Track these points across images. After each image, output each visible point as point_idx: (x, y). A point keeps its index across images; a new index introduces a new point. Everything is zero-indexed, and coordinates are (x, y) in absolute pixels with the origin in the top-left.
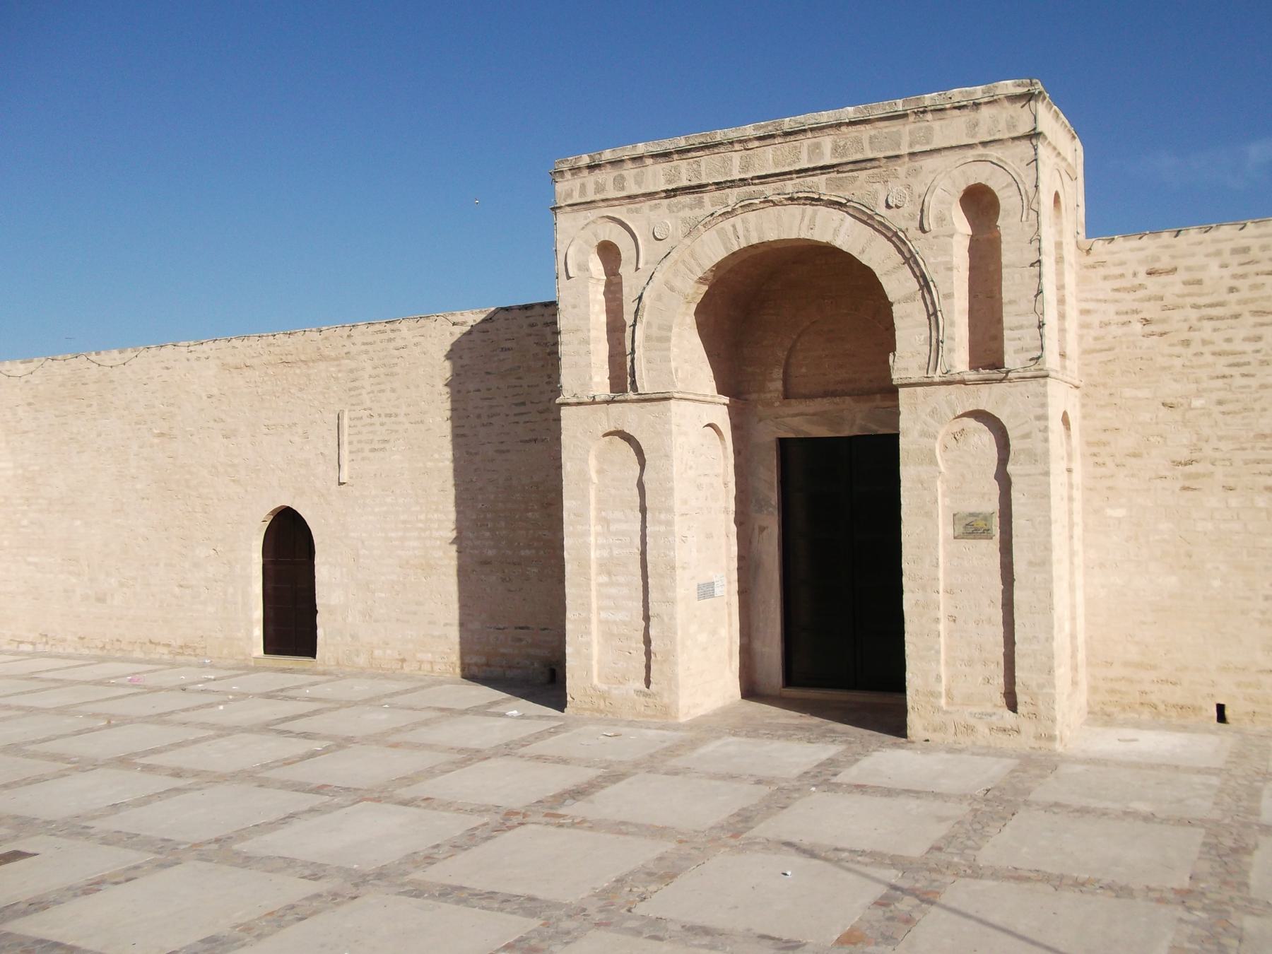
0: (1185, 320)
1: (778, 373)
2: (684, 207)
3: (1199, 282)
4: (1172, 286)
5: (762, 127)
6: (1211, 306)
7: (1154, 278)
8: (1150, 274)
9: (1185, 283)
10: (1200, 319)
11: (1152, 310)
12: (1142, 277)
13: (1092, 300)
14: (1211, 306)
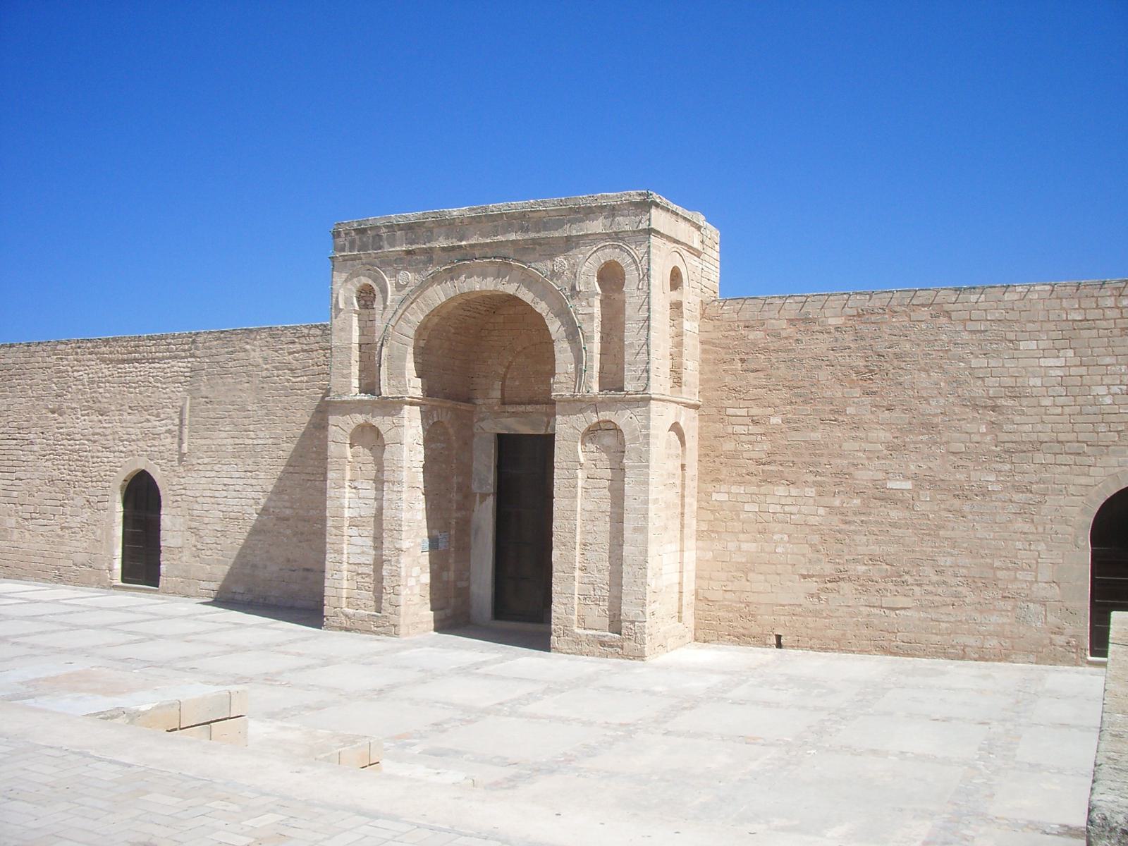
1: (498, 385)
2: (420, 262)
5: (474, 209)
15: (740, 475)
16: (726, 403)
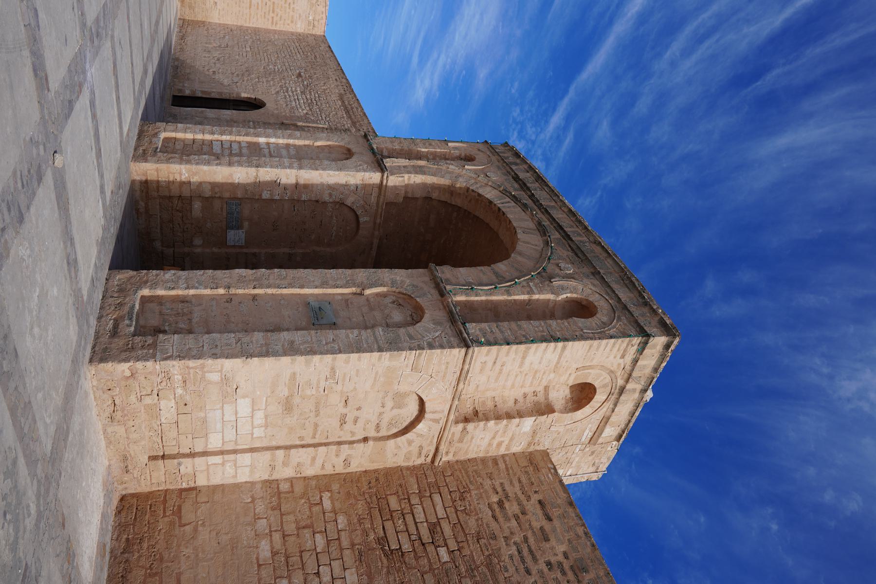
0: (512, 533)
3: (547, 539)
4: (537, 520)
6: (531, 551)
7: (538, 506)
8: (540, 502)
9: (542, 528)
10: (515, 543)
11: (512, 508)
12: (535, 498)
13: (506, 465)
14: (531, 551)
15: (360, 521)
16: (445, 491)
